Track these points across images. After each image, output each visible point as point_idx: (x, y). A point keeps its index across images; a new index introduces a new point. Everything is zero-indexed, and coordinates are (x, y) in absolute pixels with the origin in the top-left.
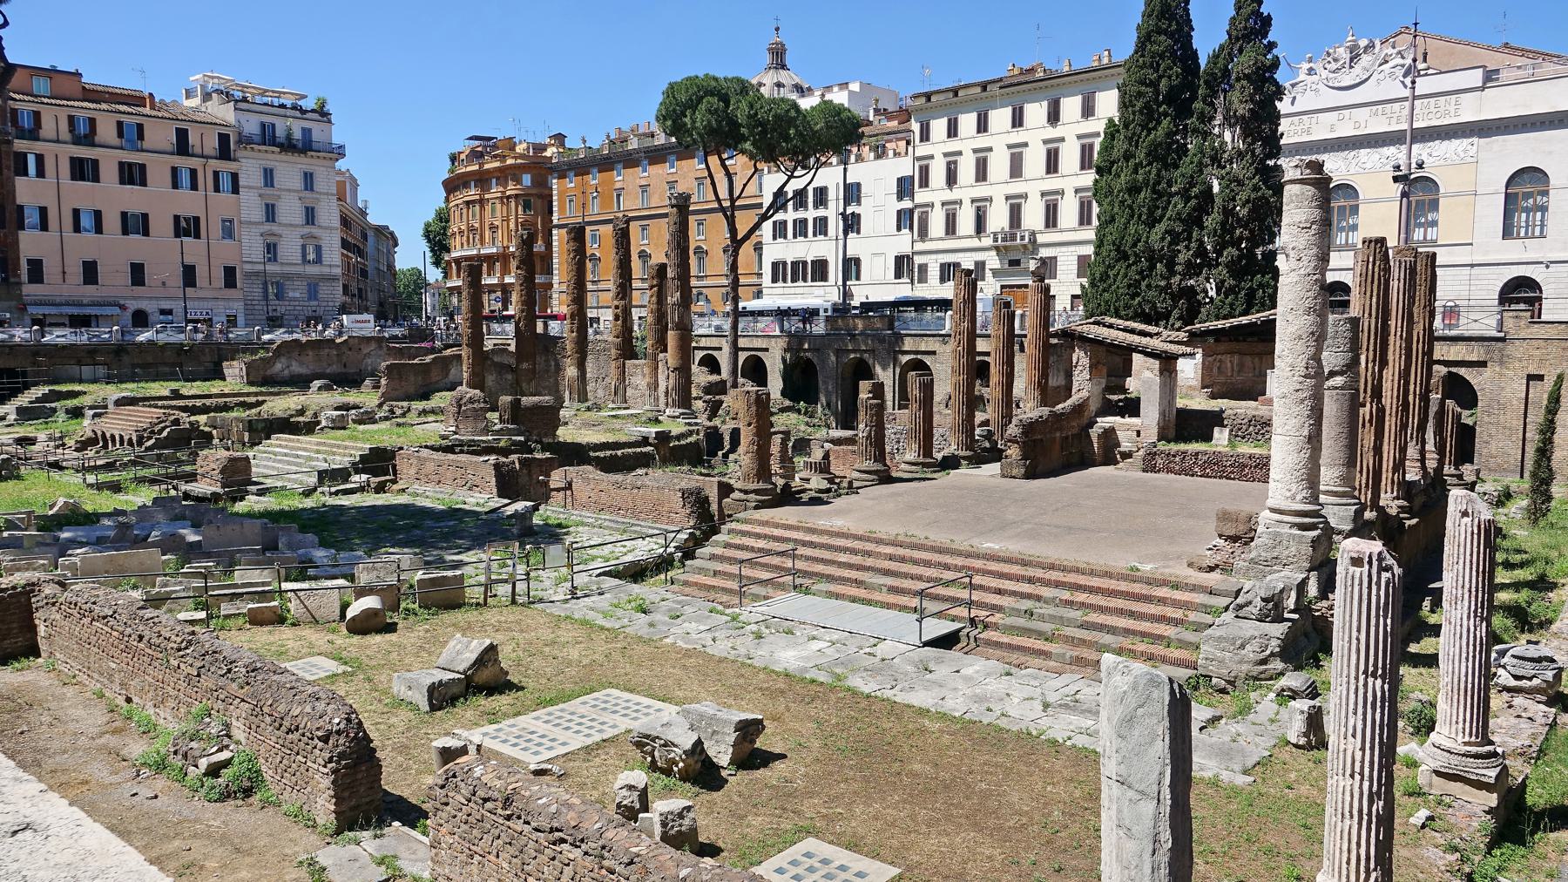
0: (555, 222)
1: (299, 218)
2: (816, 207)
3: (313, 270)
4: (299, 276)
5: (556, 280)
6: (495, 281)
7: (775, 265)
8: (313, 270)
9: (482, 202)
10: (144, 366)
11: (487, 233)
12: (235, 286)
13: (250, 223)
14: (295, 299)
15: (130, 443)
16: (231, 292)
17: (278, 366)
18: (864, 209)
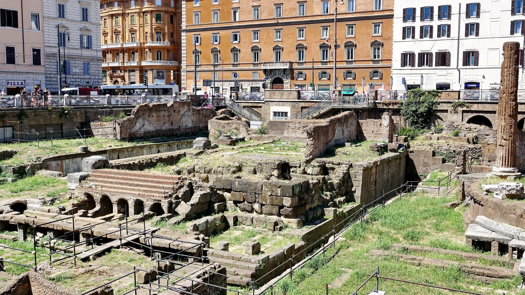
0: (184, 28)
1: (78, 16)
2: (440, 18)
3: (86, 53)
4: (81, 57)
5: (184, 64)
6: (135, 64)
7: (404, 56)
8: (86, 53)
9: (123, 15)
10: (38, 127)
11: (127, 34)
12: (40, 64)
13: (49, 18)
14: (76, 74)
15: (157, 209)
16: (37, 69)
17: (138, 125)
18: (483, 21)
